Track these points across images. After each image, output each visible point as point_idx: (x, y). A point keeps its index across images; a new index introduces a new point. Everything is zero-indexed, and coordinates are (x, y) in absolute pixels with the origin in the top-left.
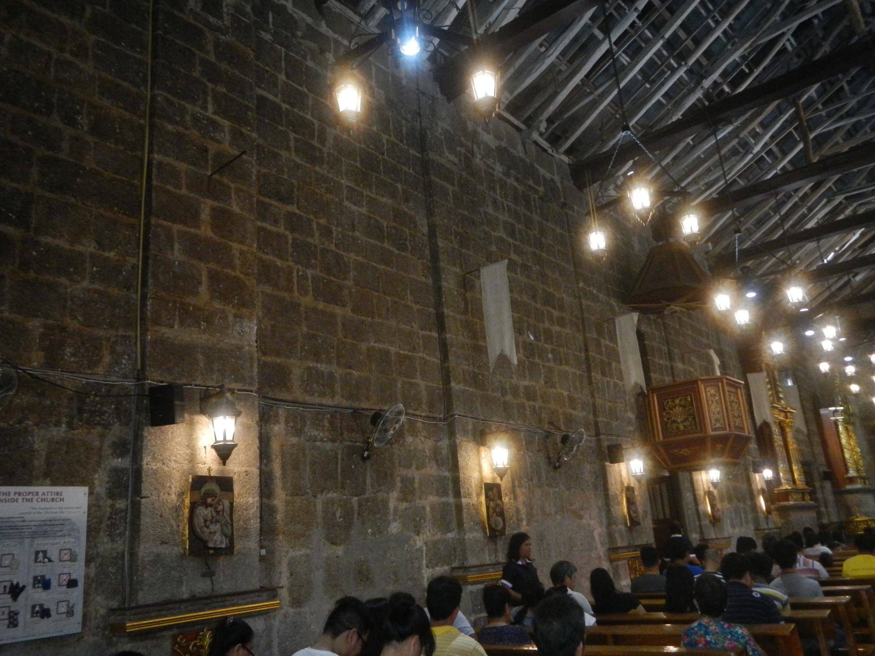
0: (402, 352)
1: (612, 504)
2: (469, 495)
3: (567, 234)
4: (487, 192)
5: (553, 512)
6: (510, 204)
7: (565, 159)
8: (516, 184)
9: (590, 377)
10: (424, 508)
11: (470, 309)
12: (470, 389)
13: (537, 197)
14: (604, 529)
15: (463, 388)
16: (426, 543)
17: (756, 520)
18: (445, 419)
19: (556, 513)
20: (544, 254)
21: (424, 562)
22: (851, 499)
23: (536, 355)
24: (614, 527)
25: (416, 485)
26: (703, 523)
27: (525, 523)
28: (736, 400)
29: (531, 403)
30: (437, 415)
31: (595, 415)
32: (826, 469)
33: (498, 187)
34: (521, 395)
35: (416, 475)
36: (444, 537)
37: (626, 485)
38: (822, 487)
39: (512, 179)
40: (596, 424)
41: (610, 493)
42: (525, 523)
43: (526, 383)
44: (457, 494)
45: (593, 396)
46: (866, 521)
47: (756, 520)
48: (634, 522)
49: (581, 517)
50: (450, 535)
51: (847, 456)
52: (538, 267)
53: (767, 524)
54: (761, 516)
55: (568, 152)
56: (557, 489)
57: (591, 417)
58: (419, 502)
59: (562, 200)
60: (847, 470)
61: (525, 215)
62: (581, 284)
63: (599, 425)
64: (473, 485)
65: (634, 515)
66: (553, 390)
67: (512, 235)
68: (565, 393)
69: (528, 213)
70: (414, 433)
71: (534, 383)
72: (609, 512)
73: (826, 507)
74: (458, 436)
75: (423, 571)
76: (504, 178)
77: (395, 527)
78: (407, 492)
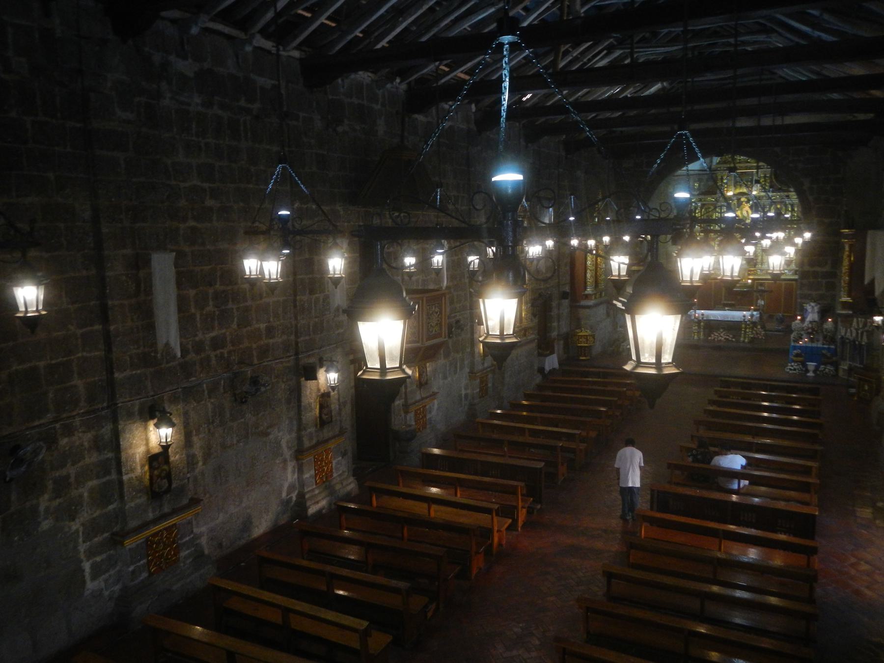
0: (53, 362)
1: (303, 413)
2: (132, 470)
5: (235, 442)
7: (296, 54)
9: (295, 301)
10: (81, 496)
11: (142, 289)
12: (139, 372)
14: (294, 435)
15: (130, 373)
16: (83, 525)
17: (472, 365)
18: (108, 407)
19: (238, 442)
21: (81, 540)
22: (583, 313)
23: (230, 300)
24: (303, 433)
25: (72, 480)
26: (409, 389)
27: (200, 463)
28: (437, 310)
29: (218, 352)
30: (100, 406)
31: (297, 336)
32: (567, 289)
34: (207, 348)
35: (71, 470)
36: (104, 511)
37: (322, 391)
38: (559, 305)
40: (297, 343)
41: (303, 404)
42: (200, 463)
43: (213, 334)
44: (120, 473)
45: (296, 318)
46: (587, 336)
47: (472, 365)
48: (323, 422)
49: (267, 434)
50: (111, 507)
51: (588, 275)
52: (242, 204)
53: (483, 364)
54: (478, 359)
55: (298, 48)
56: (243, 420)
57: (293, 337)
58: (74, 493)
60: (585, 288)
63: (299, 345)
64: (138, 460)
65: (324, 417)
66: (249, 328)
68: (263, 326)
70: (69, 430)
71: (223, 331)
72: (300, 420)
73: (559, 321)
74: (121, 422)
75: (79, 548)
77: (46, 525)
78: (63, 485)
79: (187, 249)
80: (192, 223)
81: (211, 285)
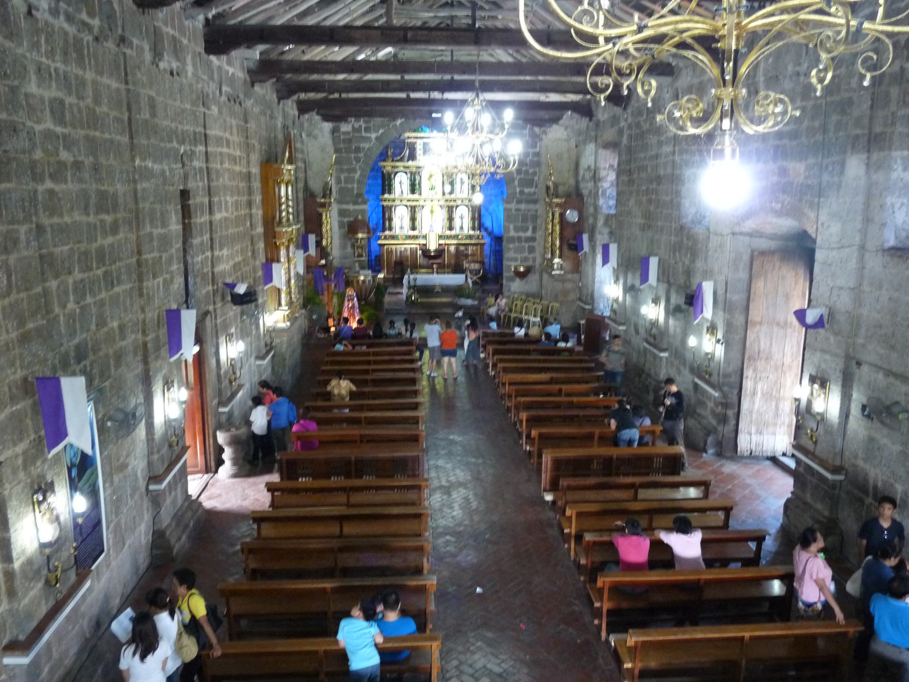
3: (123, 87)
4: (28, 55)
6: (58, 65)
8: (66, 26)
12: (18, 407)
13: (91, 38)
20: (97, 134)
33: (43, 41)
39: (62, 18)
57: (140, 336)
59: (120, 31)
61: (77, 76)
62: (137, 162)
67: (61, 121)
68: (115, 324)
69: (80, 73)
74: (7, 486)
76: (51, 19)
79: (46, 221)
80: (49, 184)
81: (70, 273)
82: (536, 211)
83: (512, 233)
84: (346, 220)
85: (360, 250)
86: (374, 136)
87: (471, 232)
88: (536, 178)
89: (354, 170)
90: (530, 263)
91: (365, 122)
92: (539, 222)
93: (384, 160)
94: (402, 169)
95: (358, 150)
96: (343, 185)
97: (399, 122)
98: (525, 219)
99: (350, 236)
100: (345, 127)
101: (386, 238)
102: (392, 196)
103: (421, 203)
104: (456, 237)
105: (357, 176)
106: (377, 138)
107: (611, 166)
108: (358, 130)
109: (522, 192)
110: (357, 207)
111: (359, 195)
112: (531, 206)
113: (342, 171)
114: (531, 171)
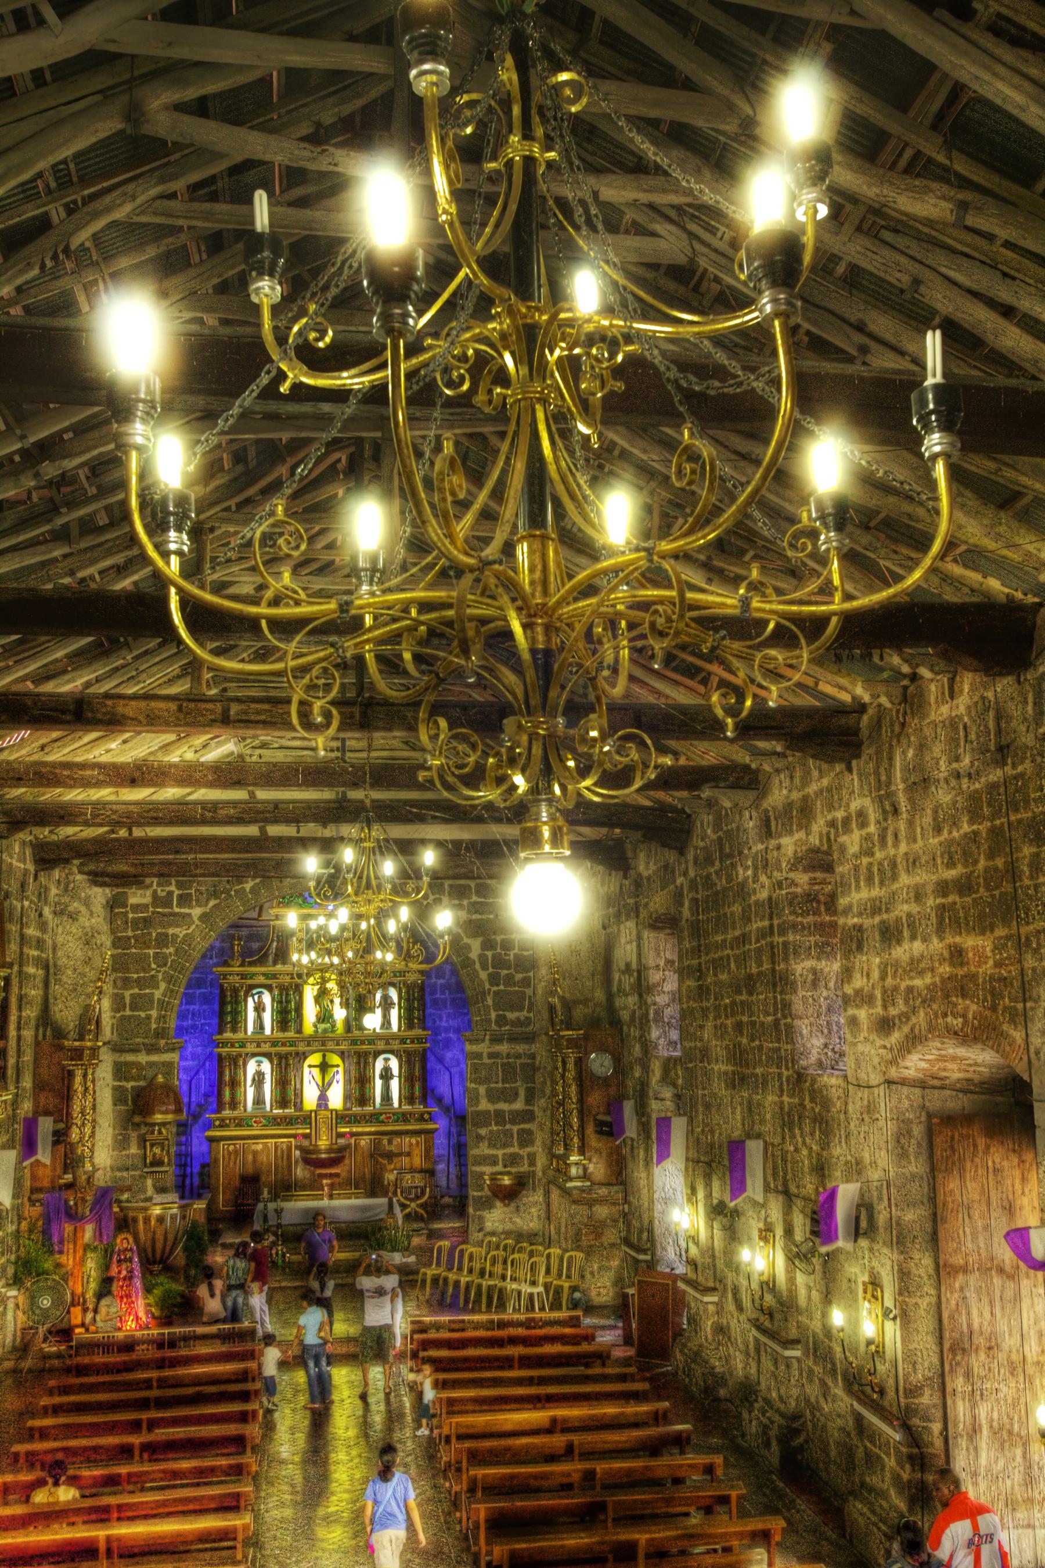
82: (533, 1057)
83: (484, 1105)
84: (129, 1085)
85: (157, 1150)
86: (196, 912)
87: (406, 1108)
88: (529, 991)
89: (153, 982)
90: (525, 1168)
91: (180, 885)
92: (539, 1078)
93: (225, 964)
94: (261, 980)
95: (163, 940)
96: (128, 1013)
97: (248, 885)
98: (509, 1072)
99: (137, 1119)
100: (137, 897)
101: (223, 1126)
102: (240, 1035)
103: (301, 1047)
104: (373, 1118)
105: (158, 994)
106: (204, 917)
107: (669, 962)
108: (167, 902)
109: (501, 1020)
110: (154, 1058)
111: (160, 1034)
112: (521, 1048)
113: (126, 983)
114: (519, 977)
